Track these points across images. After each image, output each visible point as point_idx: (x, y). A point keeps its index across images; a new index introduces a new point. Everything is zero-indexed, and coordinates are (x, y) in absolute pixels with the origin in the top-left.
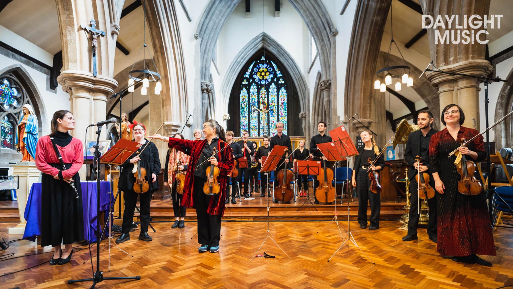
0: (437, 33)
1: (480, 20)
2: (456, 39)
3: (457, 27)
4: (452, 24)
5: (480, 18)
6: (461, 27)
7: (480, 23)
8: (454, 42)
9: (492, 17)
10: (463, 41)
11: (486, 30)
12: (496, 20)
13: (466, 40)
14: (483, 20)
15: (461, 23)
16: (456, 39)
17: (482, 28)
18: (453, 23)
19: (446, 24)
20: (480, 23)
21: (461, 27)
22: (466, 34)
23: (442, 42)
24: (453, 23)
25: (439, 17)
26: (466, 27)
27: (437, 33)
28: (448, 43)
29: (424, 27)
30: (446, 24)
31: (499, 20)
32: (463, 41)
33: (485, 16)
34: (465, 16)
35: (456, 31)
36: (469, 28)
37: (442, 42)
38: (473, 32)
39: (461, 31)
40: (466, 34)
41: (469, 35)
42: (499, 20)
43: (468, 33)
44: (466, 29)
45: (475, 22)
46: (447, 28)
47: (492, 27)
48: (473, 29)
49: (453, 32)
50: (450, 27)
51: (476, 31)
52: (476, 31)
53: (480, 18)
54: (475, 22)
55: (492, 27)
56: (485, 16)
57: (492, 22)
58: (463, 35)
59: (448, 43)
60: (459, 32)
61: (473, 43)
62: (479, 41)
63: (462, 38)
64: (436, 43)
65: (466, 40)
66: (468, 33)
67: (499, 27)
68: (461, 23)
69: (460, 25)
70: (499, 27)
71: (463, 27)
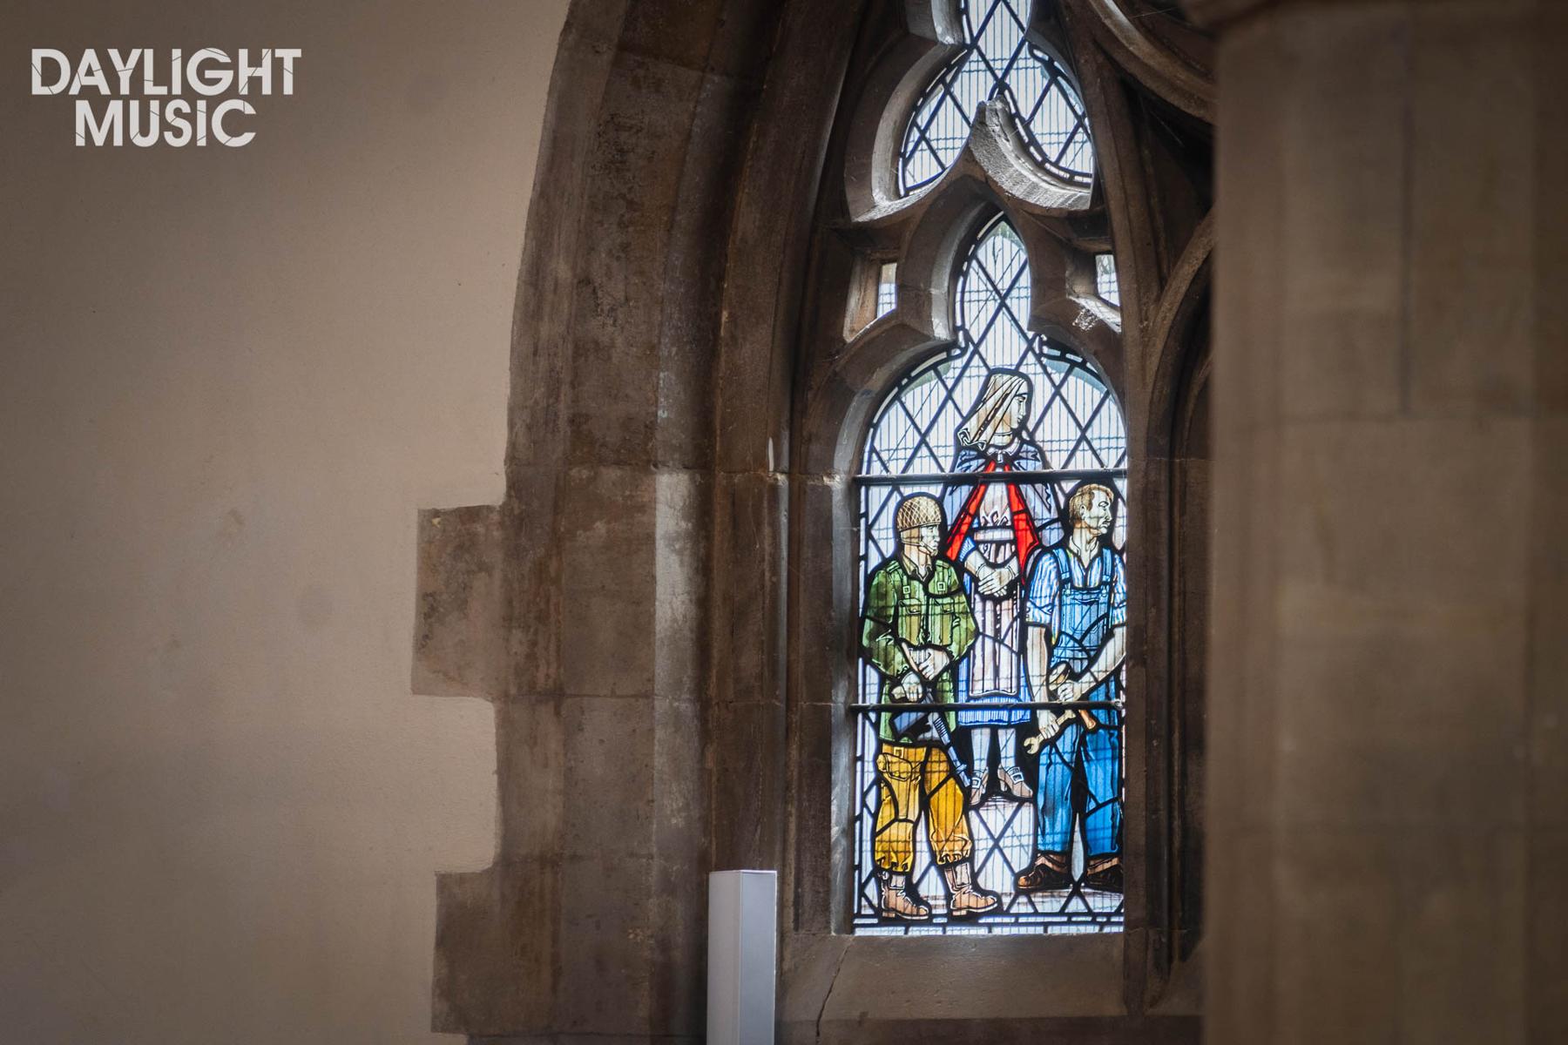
0: (83, 109)
1: (224, 67)
2: (144, 131)
3: (149, 88)
4: (132, 78)
5: (227, 60)
6: (163, 90)
7: (227, 77)
8: (140, 141)
9: (267, 55)
10: (168, 136)
11: (243, 98)
12: (277, 64)
13: (178, 133)
14: (233, 66)
15: (163, 77)
16: (144, 131)
17: (232, 92)
18: (137, 78)
19: (112, 77)
20: (227, 77)
21: (163, 90)
22: (178, 112)
23: (99, 139)
24: (137, 78)
25: (90, 57)
26: (177, 90)
27: (83, 109)
28: (118, 141)
29: (38, 89)
30: (112, 77)
31: (288, 65)
32: (168, 136)
33: (243, 54)
34: (177, 53)
35: (145, 102)
36: (189, 94)
37: (99, 139)
38: (201, 105)
39: (164, 101)
40: (178, 112)
41: (191, 117)
42: (288, 65)
43: (186, 108)
44: (177, 97)
45: (209, 74)
46: (115, 94)
47: (267, 89)
48: (202, 97)
49: (134, 105)
50: (125, 89)
51: (213, 102)
52: (213, 102)
53: (223, 58)
54: (209, 74)
55: (267, 89)
56: (243, 54)
57: (265, 72)
58: (170, 116)
59: (118, 141)
60: (155, 106)
61: (202, 142)
62: (221, 136)
63: (165, 125)
64: (80, 142)
65: (178, 133)
66: (186, 108)
67: (288, 89)
68: (163, 77)
69: (156, 83)
70: (288, 89)
71: (170, 90)
